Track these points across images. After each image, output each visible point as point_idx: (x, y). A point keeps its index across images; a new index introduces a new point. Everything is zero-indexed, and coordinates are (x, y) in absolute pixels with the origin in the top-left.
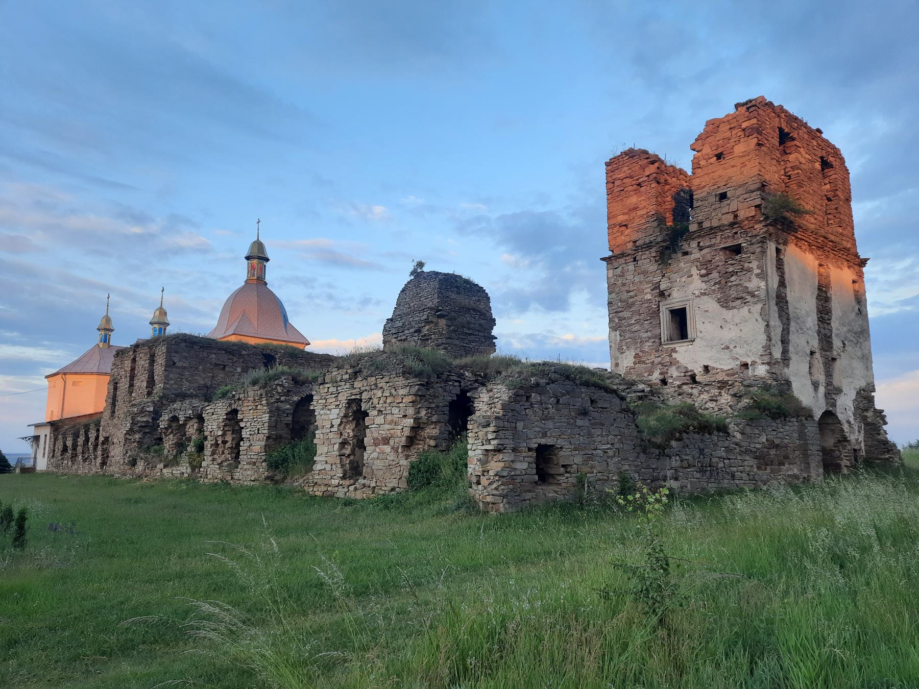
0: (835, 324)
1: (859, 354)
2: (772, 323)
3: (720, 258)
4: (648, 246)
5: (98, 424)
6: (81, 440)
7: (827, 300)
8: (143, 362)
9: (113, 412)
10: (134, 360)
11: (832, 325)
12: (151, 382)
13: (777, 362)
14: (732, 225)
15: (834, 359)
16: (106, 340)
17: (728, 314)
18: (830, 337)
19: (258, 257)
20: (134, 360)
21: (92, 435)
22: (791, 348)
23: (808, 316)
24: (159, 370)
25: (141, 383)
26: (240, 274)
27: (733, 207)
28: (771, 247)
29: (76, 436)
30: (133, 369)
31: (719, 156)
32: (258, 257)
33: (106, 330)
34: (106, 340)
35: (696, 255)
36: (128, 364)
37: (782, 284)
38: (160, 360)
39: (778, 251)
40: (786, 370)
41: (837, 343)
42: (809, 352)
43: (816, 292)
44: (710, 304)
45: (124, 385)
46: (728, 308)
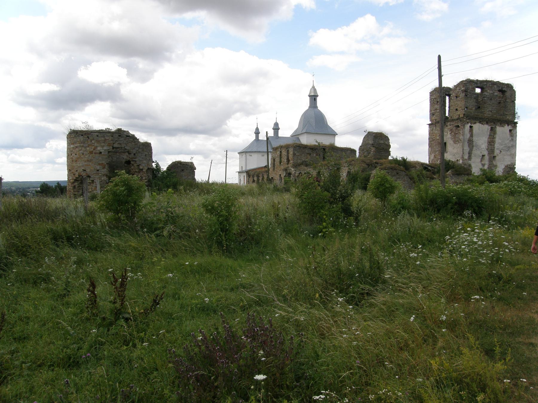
0: (496, 146)
1: (509, 153)
2: (465, 148)
3: (455, 128)
4: (438, 122)
5: (268, 171)
6: (261, 178)
7: (494, 138)
8: (284, 153)
9: (274, 169)
10: (281, 152)
11: (496, 145)
12: (288, 160)
13: (466, 160)
14: (457, 119)
15: (494, 157)
16: (257, 137)
17: (455, 145)
18: (494, 150)
19: (314, 98)
20: (281, 152)
21: (265, 177)
22: (472, 155)
23: (482, 144)
24: (291, 156)
25: (284, 160)
26: (306, 104)
27: (459, 113)
28: (468, 126)
29: (258, 176)
30: (281, 155)
31: (457, 97)
32: (314, 98)
33: (257, 133)
34: (257, 137)
35: (449, 127)
36: (278, 153)
37: (472, 136)
38: (291, 152)
39: (471, 127)
40: (470, 162)
41: (497, 152)
42: (481, 155)
43: (488, 137)
44: (452, 142)
45: (277, 160)
46: (455, 143)
